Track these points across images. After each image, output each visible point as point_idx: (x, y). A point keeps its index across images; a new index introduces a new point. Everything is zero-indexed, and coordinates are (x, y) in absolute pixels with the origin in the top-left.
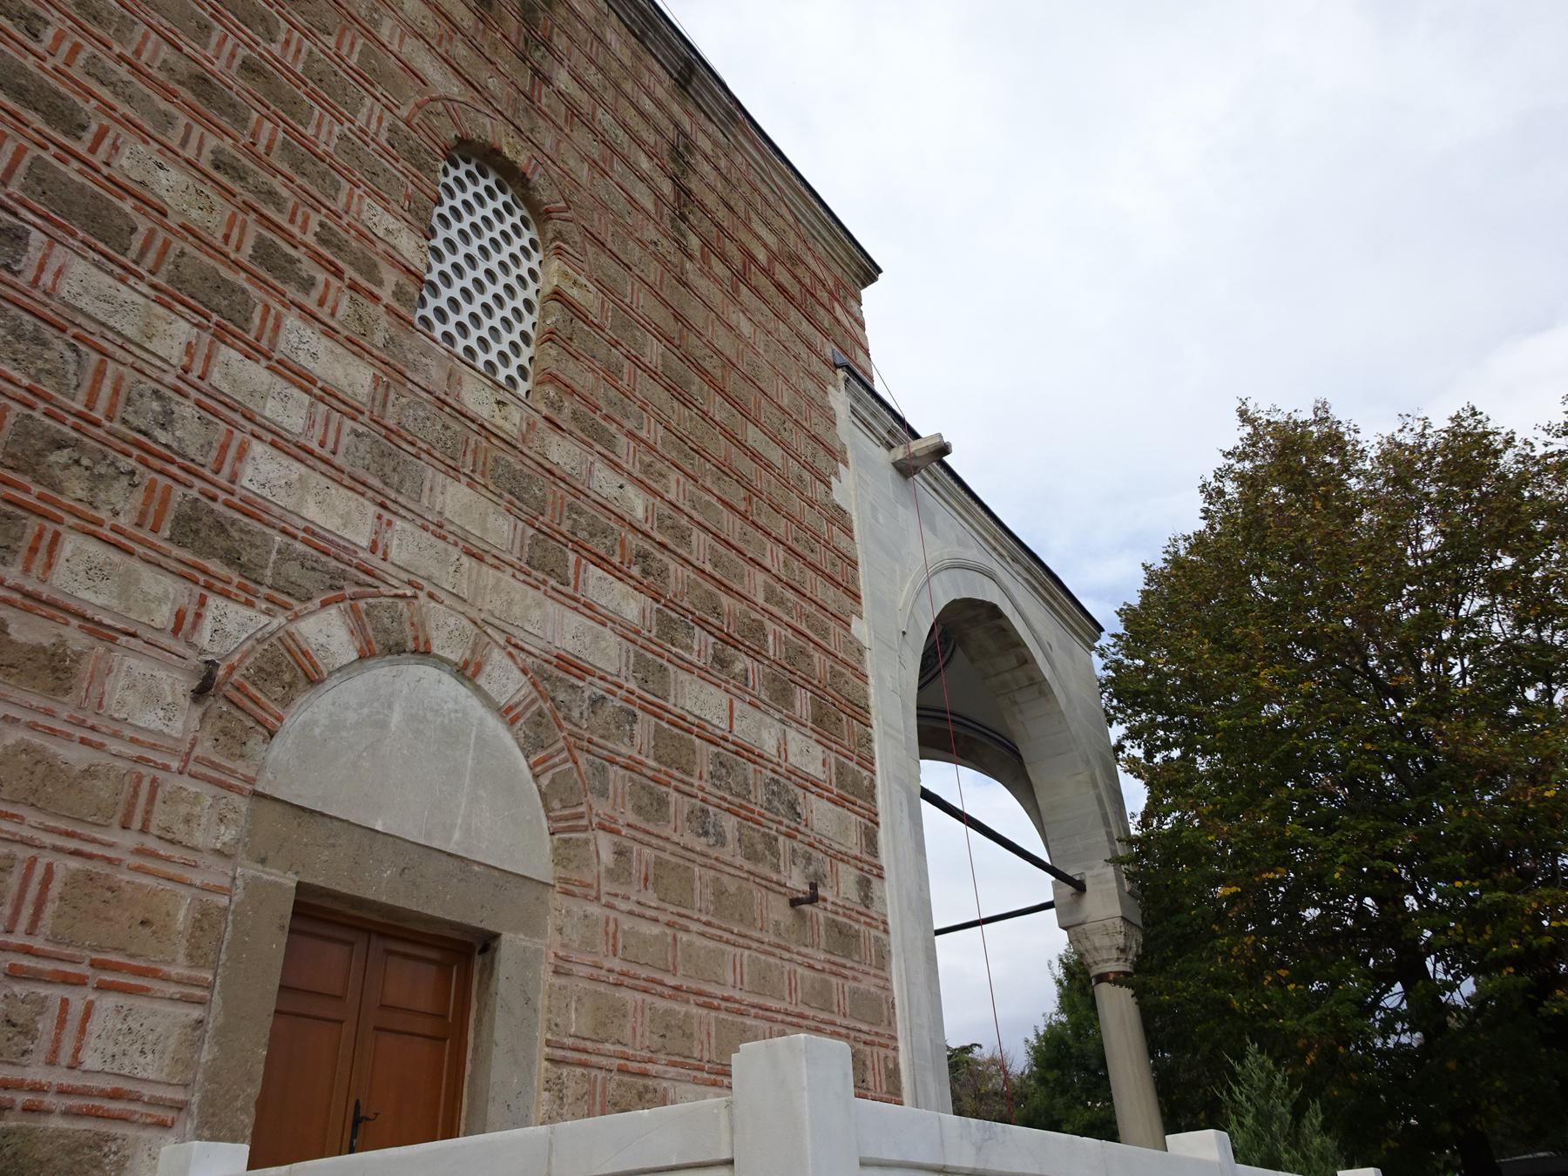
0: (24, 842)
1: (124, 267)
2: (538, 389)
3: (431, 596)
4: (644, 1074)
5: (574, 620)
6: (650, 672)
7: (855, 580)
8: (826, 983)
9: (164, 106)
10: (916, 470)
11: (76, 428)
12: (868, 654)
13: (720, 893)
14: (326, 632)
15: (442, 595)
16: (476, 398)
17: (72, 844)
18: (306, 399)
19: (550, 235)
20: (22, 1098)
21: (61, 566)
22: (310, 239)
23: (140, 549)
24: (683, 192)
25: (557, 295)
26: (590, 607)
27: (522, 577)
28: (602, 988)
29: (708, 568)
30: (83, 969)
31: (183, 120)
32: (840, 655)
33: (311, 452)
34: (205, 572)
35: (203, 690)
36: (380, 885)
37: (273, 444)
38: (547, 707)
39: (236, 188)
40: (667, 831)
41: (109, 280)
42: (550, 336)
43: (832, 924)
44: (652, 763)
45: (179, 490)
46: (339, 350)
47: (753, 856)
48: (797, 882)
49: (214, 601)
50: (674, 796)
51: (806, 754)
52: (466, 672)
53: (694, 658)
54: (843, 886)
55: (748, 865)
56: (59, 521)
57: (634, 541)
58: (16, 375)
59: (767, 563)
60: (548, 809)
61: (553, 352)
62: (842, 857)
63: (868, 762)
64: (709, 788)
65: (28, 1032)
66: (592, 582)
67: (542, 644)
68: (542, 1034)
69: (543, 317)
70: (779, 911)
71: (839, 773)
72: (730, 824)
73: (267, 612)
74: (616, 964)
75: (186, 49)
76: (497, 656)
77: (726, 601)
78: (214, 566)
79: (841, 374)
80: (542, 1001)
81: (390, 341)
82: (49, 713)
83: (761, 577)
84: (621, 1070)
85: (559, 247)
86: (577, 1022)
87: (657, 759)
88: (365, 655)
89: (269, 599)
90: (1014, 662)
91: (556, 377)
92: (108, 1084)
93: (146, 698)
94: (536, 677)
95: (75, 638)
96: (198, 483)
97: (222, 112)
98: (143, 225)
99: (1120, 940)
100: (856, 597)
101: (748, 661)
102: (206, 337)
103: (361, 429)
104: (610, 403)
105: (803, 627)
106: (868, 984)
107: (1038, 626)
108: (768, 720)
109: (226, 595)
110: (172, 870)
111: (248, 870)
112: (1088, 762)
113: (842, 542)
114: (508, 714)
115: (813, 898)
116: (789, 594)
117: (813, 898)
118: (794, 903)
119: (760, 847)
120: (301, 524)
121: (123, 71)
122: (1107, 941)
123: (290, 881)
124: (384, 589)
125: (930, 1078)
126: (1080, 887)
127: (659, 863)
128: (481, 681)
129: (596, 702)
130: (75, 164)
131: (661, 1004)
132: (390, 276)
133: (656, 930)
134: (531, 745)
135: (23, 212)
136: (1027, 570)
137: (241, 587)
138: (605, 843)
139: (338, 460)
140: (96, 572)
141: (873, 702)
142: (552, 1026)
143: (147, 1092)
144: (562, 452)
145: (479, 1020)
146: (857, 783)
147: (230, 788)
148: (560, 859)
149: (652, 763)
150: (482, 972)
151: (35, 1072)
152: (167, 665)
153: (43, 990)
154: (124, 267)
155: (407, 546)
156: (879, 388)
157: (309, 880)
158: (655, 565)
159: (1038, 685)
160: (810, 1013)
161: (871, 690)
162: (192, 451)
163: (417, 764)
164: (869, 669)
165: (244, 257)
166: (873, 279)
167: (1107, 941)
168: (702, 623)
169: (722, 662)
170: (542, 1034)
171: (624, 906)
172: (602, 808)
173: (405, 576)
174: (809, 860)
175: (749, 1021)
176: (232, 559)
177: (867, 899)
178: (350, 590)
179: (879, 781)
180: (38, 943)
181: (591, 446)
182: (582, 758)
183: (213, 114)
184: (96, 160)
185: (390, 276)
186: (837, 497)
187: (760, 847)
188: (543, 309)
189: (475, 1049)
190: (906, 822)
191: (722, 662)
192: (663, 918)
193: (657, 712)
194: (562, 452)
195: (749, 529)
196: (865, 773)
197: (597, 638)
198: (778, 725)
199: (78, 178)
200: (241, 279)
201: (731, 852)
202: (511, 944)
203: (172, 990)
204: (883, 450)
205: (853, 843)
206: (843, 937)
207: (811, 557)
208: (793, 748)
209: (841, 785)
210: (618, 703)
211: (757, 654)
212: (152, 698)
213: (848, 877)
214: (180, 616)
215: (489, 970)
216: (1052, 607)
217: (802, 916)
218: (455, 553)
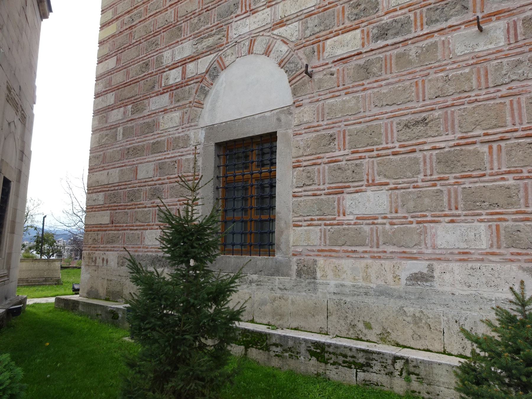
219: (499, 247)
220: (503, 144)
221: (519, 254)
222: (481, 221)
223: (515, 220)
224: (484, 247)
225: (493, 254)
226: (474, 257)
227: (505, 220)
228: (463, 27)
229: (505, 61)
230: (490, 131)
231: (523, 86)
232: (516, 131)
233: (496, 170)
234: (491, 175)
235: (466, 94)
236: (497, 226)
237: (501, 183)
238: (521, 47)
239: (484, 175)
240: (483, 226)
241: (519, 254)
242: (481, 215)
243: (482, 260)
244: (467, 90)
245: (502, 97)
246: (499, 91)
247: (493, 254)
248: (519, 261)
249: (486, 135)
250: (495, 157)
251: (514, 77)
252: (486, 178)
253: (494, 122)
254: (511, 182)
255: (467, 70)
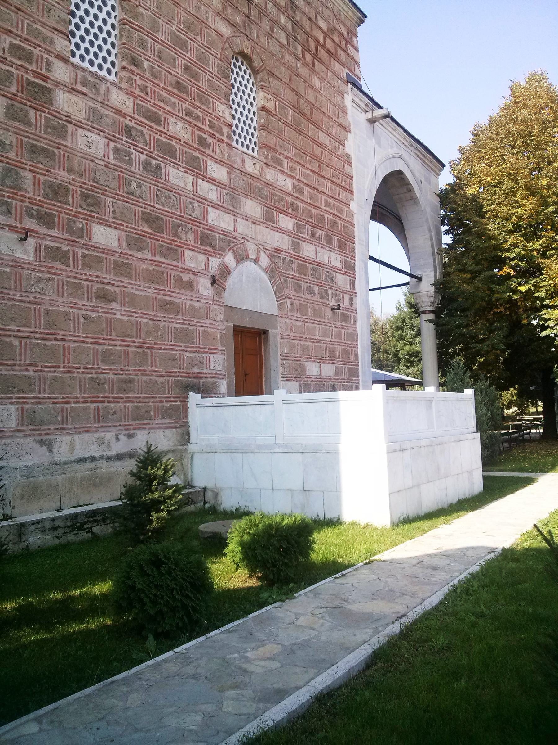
0: (195, 326)
1: (178, 165)
2: (261, 150)
3: (247, 240)
4: (300, 361)
5: (277, 235)
6: (296, 246)
7: (351, 185)
8: (340, 331)
9: (173, 100)
10: (375, 122)
11: (181, 220)
12: (355, 215)
13: (315, 310)
14: (229, 259)
15: (249, 239)
16: (249, 167)
17: (201, 324)
18: (215, 188)
19: (258, 80)
20: (204, 375)
21: (186, 259)
22: (207, 128)
23: (197, 249)
24: (295, 23)
25: (263, 108)
26: (280, 229)
27: (265, 225)
28: (290, 341)
29: (309, 201)
30: (207, 350)
31: (177, 102)
32: (346, 219)
33: (218, 205)
34: (207, 251)
35: (214, 282)
36: (246, 323)
37: (212, 206)
38: (273, 265)
39: (190, 120)
40: (302, 295)
41: (176, 171)
42: (263, 127)
43: (342, 313)
44: (297, 275)
45: (199, 229)
46: (219, 166)
47: (322, 297)
48: (333, 303)
49: (210, 258)
50: (303, 284)
51: (336, 260)
52: (256, 261)
53: (305, 236)
54: (345, 302)
55: (321, 300)
56: (183, 247)
57: (290, 199)
58: (168, 210)
59: (325, 191)
60: (276, 295)
61: (264, 134)
62: (345, 292)
63: (353, 258)
64: (311, 279)
65: (203, 363)
66: (280, 220)
67: (271, 246)
68: (279, 353)
69: (260, 118)
70: (329, 313)
71: (345, 264)
72: (316, 288)
73: (219, 258)
74: (292, 334)
75: (173, 72)
76: (262, 254)
77: (314, 211)
78: (209, 248)
79: (350, 86)
80: (279, 346)
81: (229, 156)
82: (192, 296)
83: (324, 197)
84: (295, 360)
85: (262, 86)
86: (286, 350)
87: (299, 273)
88: (238, 263)
89: (219, 254)
90: (405, 190)
91: (266, 145)
92: (215, 372)
93: (204, 287)
94: (271, 257)
95: (192, 277)
96: (202, 226)
97: (183, 92)
98: (178, 147)
99: (432, 299)
100: (351, 192)
101: (320, 231)
102: (195, 178)
103: (227, 192)
104: (280, 147)
105: (336, 213)
106: (351, 330)
107: (417, 174)
108: (326, 251)
109: (211, 256)
110: (215, 327)
111: (226, 324)
112: (430, 230)
113: (348, 170)
114: (266, 270)
115: (339, 309)
116: (332, 201)
117: (339, 309)
118: (333, 309)
119: (324, 294)
120: (221, 229)
121: (163, 93)
122: (427, 299)
123: (232, 325)
124: (238, 242)
125: (366, 355)
126: (420, 279)
127: (301, 304)
128: (260, 263)
129: (284, 260)
130: (163, 135)
131: (302, 343)
132: (225, 130)
133: (300, 323)
134: (272, 277)
135: (159, 159)
136: (416, 149)
137: (214, 253)
138: (288, 301)
139: (224, 205)
140: (192, 259)
141: (356, 234)
142: (282, 351)
143: (220, 373)
144: (270, 175)
145: (265, 351)
146: (350, 266)
147: (220, 306)
148: (280, 309)
149: (297, 275)
150: (264, 339)
151: (205, 371)
152: (206, 278)
153: (203, 355)
154: (178, 165)
155: (242, 227)
156: (364, 88)
157: (237, 324)
158: (295, 206)
159: (414, 200)
160: (336, 340)
161: (356, 230)
162: (199, 217)
163: (251, 291)
164: (355, 222)
165: (196, 146)
166: (363, 22)
167: (427, 299)
168: (308, 223)
169: (313, 235)
170: (279, 353)
171: (293, 318)
172: (287, 292)
173: (242, 236)
174: (336, 295)
175: (322, 345)
176: (211, 245)
177: (351, 304)
178: (232, 245)
179: (356, 263)
180: (201, 346)
181: (276, 168)
182: (282, 278)
183: (182, 95)
184: (165, 131)
185: (225, 130)
186: (347, 150)
187: (324, 294)
188: (259, 114)
189: (265, 357)
190: (364, 274)
191: (313, 235)
192: (302, 320)
193: (298, 258)
194: (270, 175)
195: (320, 179)
196: (353, 261)
197: (283, 239)
198: (329, 252)
199: (164, 140)
200: (196, 154)
201: (317, 298)
202: (272, 332)
203: (220, 352)
204: (363, 113)
205: (348, 287)
206: (345, 318)
207: (338, 182)
208: (332, 259)
209: (345, 268)
210: (289, 258)
211: (322, 228)
212: (205, 287)
213: (347, 297)
214: (205, 265)
215: (267, 339)
216: (424, 162)
217: (334, 313)
218: (250, 223)
219: (22, 425)
220: (28, 341)
221: (34, 430)
222: (12, 403)
223: (33, 403)
224: (13, 425)
225: (19, 431)
226: (7, 434)
227: (27, 403)
228: (7, 229)
229: (33, 273)
230: (22, 329)
231: (42, 299)
232: (36, 333)
233: (23, 362)
234: (20, 365)
235: (7, 291)
236: (22, 408)
237: (26, 373)
238: (42, 266)
239: (15, 365)
240: (13, 408)
241: (34, 430)
242: (11, 398)
243: (12, 436)
244: (8, 287)
245: (30, 302)
246: (28, 297)
247: (19, 431)
248: (34, 435)
249: (19, 331)
250: (23, 351)
251: (38, 290)
252: (17, 368)
253: (24, 322)
254: (31, 373)
255: (8, 270)
